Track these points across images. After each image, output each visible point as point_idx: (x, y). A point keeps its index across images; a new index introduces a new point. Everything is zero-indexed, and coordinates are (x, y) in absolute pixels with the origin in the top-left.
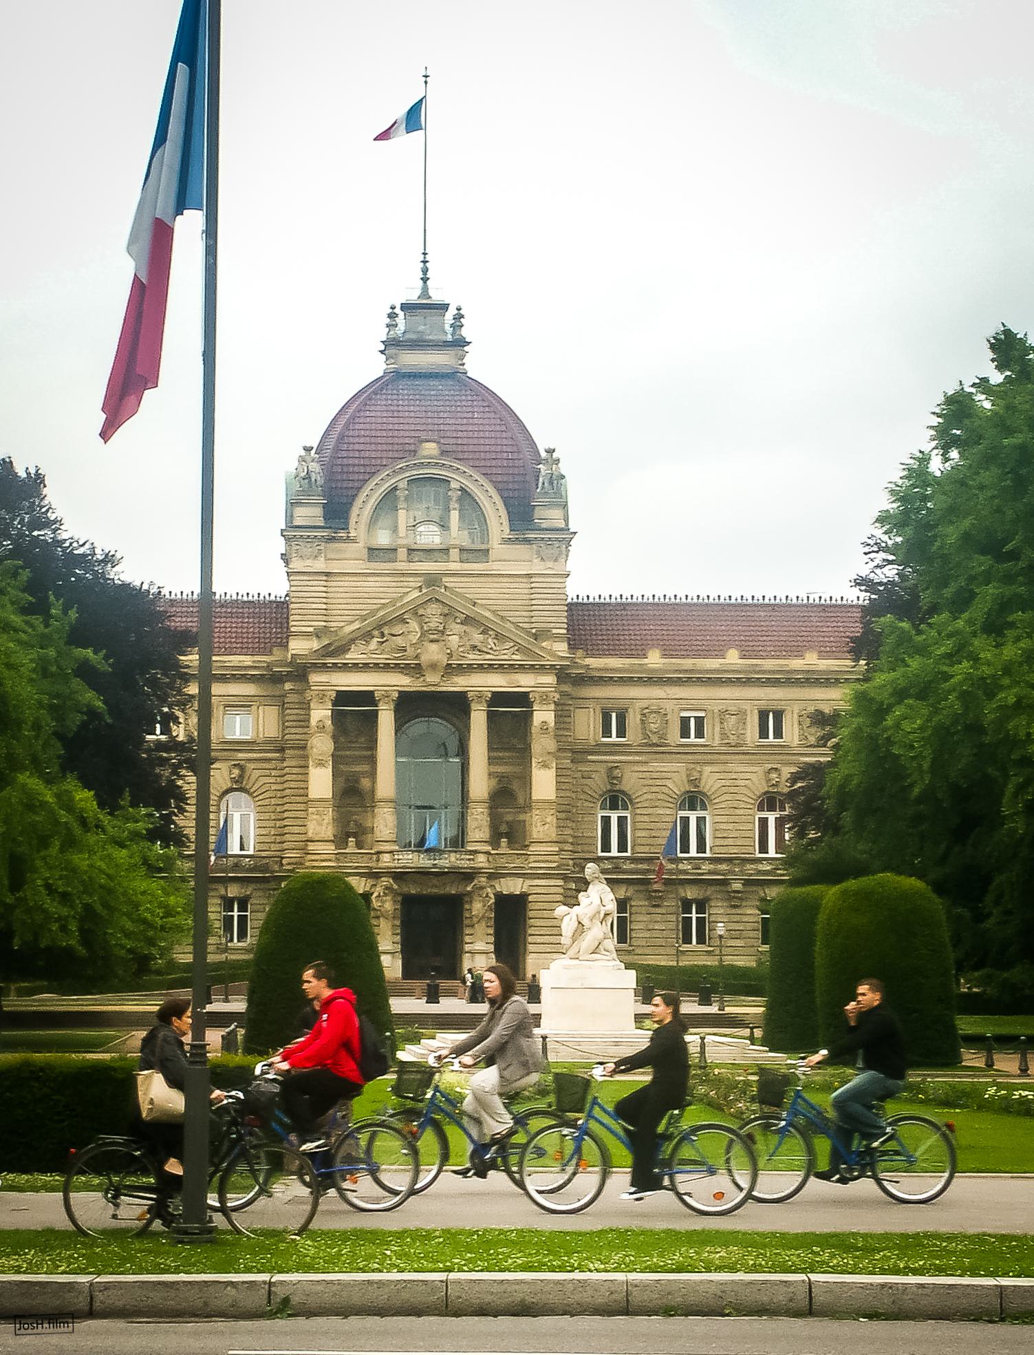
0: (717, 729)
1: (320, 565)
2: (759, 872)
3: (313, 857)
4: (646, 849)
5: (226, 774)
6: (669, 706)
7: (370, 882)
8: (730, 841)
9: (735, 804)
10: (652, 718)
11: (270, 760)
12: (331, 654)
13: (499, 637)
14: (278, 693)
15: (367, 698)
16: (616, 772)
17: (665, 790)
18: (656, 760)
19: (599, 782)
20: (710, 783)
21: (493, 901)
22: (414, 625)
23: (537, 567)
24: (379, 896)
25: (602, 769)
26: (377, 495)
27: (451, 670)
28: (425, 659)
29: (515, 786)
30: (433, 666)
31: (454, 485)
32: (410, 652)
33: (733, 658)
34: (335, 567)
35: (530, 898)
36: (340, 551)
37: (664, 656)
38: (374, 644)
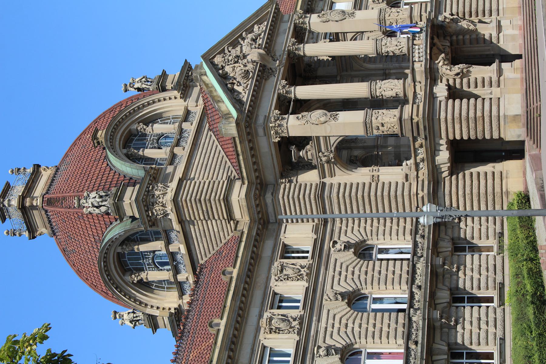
13: (250, 30)
32: (250, 67)
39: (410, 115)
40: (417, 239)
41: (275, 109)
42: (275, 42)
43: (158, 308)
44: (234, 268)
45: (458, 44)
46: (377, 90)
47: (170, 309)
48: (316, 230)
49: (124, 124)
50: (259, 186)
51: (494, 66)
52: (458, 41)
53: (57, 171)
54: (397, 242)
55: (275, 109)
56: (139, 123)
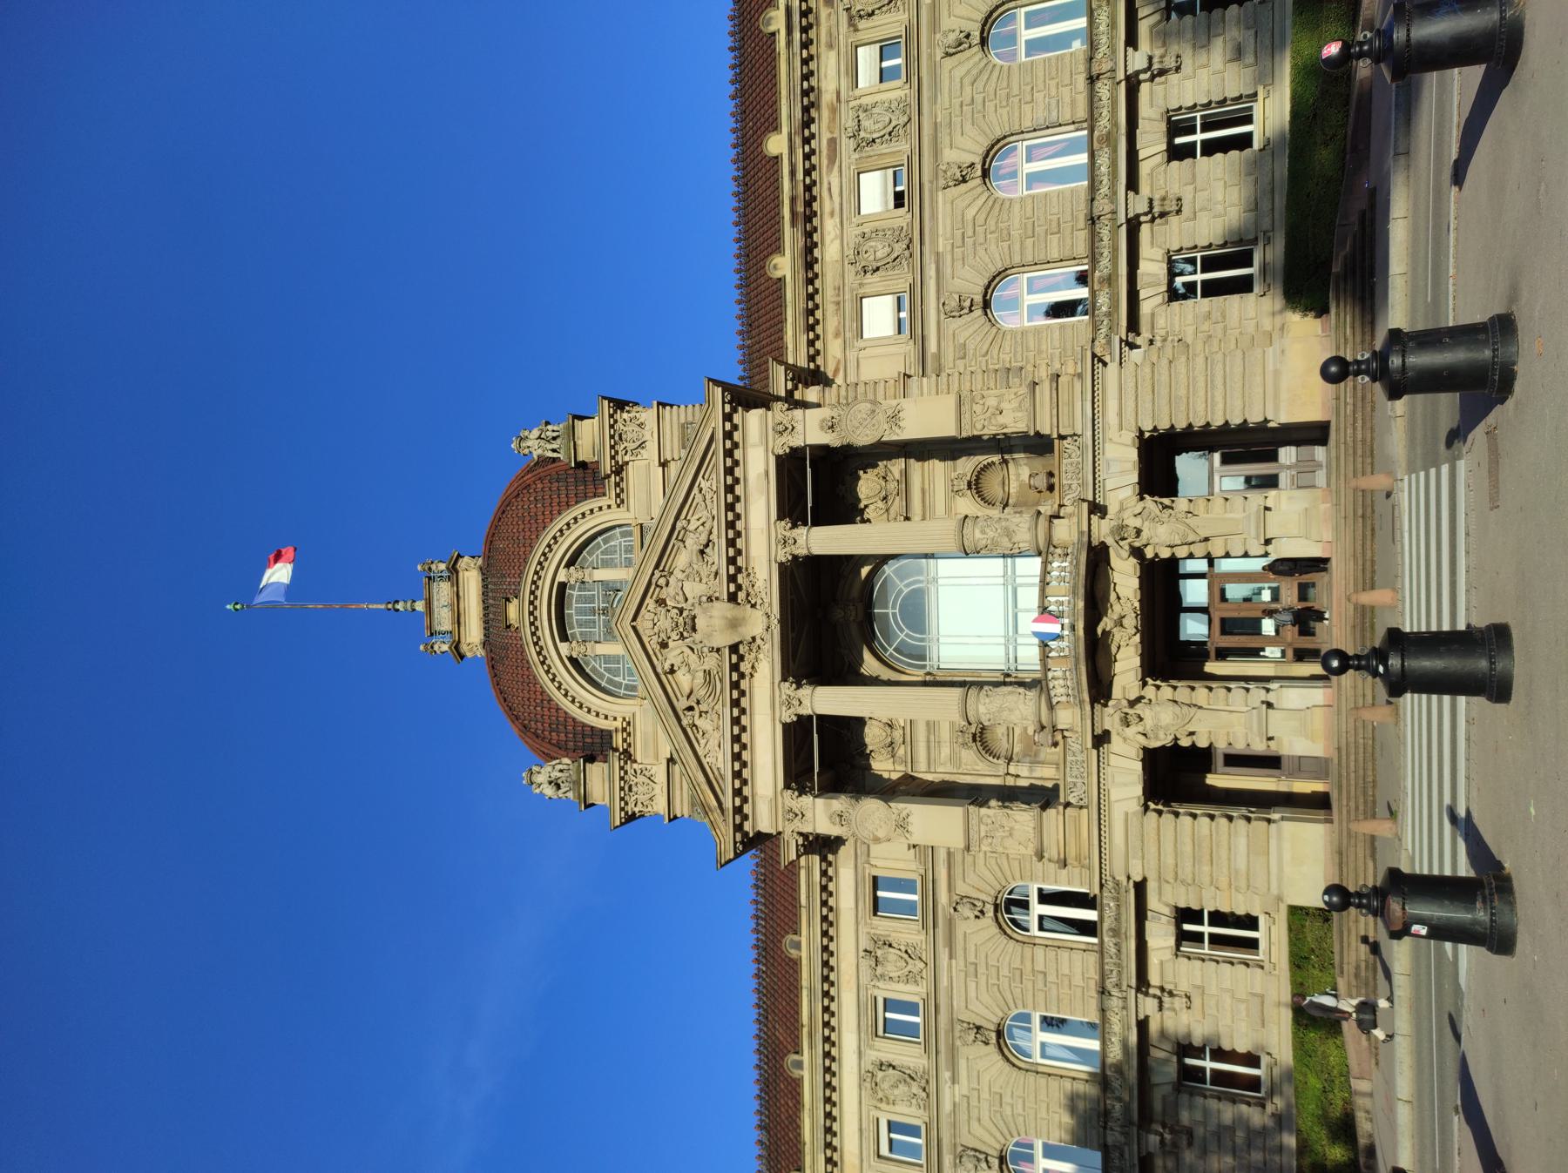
0: (885, 149)
2: (1113, 25)
4: (1082, 236)
6: (852, 233)
8: (1065, 92)
9: (1002, 93)
10: (868, 259)
16: (954, 304)
17: (980, 220)
18: (934, 242)
19: (970, 328)
20: (969, 144)
23: (651, 452)
25: (954, 324)
28: (724, 640)
33: (776, 144)
37: (779, 249)
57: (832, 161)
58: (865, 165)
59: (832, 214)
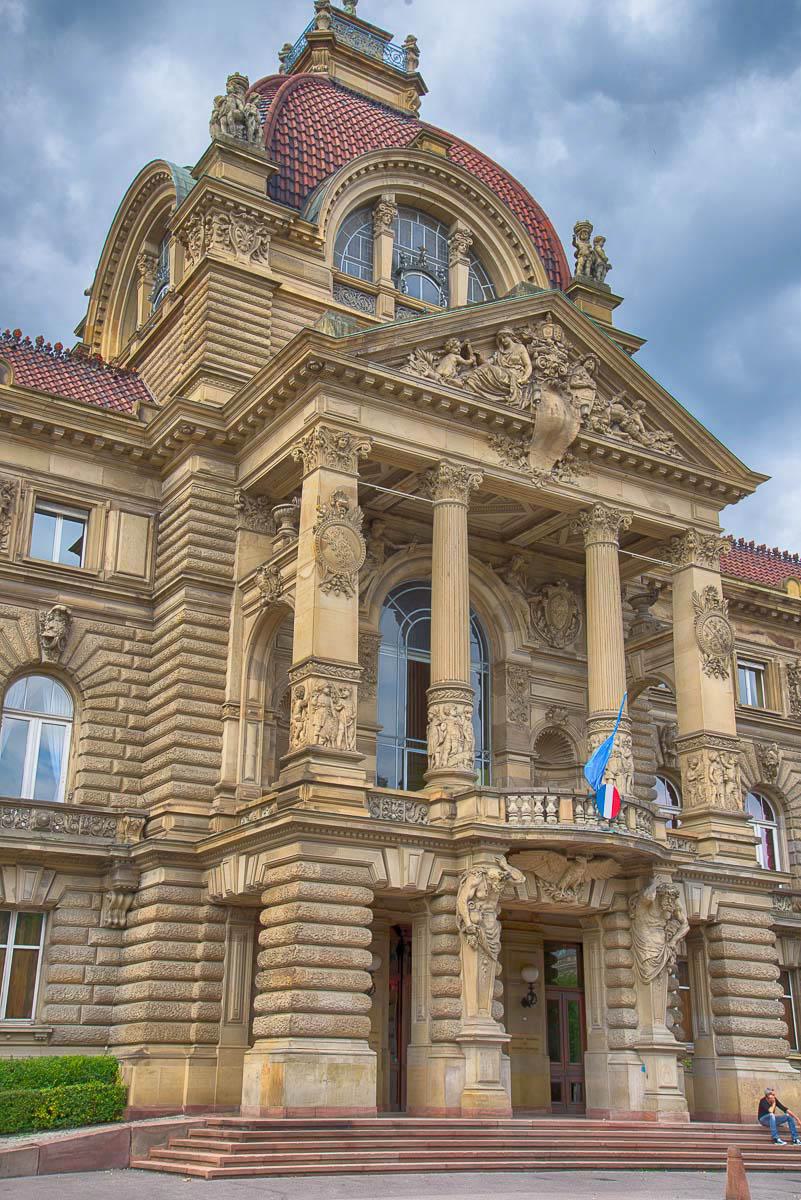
1: (262, 268)
3: (323, 792)
5: (27, 625)
7: (443, 864)
11: (122, 618)
12: (379, 358)
13: (653, 419)
14: (148, 494)
15: (421, 473)
21: (686, 929)
22: (519, 351)
24: (473, 899)
26: (347, 201)
27: (582, 455)
29: (571, 730)
30: (553, 434)
31: (461, 225)
34: (289, 286)
35: (726, 931)
36: (291, 260)
38: (448, 366)
39: (319, 779)
40: (34, 812)
41: (374, 446)
42: (622, 479)
43: (101, 322)
44: (12, 386)
45: (608, 930)
46: (442, 706)
47: (98, 345)
48: (123, 580)
49: (467, 205)
50: (220, 438)
51: (498, 1030)
52: (613, 929)
53: (403, 115)
54: (73, 769)
55: (374, 446)
56: (473, 237)
57: (777, 640)
58: (772, 672)
59: (740, 630)
